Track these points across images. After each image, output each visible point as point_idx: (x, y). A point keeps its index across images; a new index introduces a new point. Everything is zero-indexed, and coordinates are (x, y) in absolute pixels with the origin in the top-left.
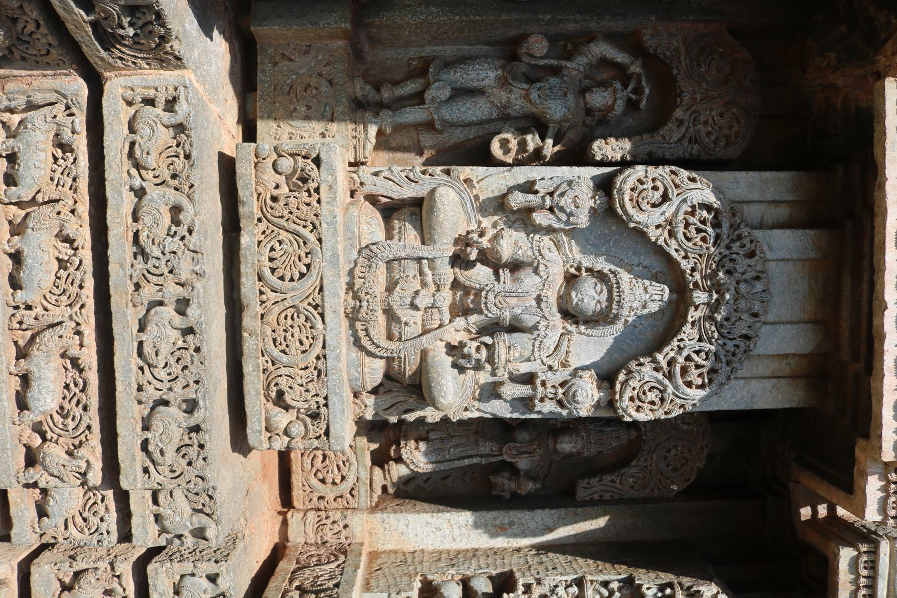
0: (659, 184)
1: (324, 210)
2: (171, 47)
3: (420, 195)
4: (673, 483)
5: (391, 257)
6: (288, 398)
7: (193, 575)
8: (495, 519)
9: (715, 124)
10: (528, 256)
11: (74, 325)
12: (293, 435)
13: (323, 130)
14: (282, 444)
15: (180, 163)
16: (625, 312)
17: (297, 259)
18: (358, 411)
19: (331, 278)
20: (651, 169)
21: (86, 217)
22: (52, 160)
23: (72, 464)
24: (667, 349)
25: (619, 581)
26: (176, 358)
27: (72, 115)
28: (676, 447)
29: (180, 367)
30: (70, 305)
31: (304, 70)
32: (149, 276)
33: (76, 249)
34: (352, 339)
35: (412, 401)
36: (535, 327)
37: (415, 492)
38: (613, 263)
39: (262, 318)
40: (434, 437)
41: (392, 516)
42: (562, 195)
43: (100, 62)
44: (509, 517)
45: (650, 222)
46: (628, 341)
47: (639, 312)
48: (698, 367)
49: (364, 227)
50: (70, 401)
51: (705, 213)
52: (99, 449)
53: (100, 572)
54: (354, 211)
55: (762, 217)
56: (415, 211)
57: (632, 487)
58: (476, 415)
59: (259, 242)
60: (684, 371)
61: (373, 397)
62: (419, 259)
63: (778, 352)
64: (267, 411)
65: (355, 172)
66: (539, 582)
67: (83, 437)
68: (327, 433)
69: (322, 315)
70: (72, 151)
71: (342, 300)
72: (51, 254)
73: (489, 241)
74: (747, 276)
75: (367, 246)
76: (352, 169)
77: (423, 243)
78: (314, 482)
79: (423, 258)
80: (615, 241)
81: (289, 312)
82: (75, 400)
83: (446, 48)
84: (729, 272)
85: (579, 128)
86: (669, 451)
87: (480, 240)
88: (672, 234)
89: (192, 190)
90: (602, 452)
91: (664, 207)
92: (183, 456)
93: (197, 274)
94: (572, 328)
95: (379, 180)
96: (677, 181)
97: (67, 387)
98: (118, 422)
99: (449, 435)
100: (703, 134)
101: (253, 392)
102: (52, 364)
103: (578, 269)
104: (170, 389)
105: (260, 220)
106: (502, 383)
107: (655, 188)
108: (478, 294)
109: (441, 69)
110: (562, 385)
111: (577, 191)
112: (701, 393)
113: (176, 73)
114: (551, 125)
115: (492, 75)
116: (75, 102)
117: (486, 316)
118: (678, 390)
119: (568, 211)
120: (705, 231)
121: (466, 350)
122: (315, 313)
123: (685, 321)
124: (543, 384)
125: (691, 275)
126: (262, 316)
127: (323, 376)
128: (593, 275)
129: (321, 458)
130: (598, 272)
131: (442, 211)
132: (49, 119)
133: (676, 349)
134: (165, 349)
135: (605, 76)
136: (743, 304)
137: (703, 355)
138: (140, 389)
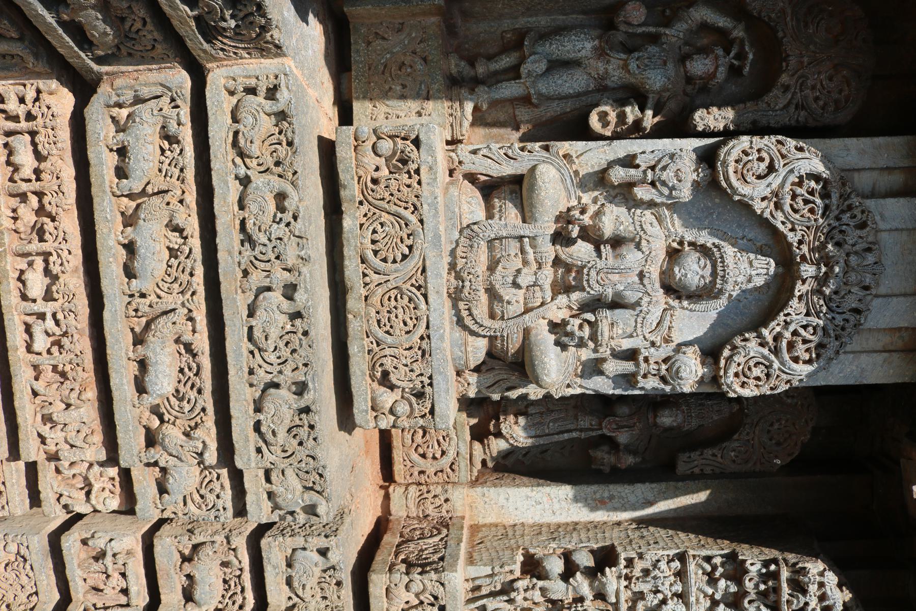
0: (764, 155)
1: (425, 191)
2: (272, 36)
3: (519, 172)
4: (776, 457)
5: (493, 236)
6: (393, 378)
7: (304, 549)
8: (595, 493)
9: (824, 88)
10: (629, 231)
11: (186, 311)
12: (399, 414)
13: (419, 109)
14: (388, 423)
15: (283, 150)
16: (729, 287)
17: (399, 240)
18: (461, 389)
19: (434, 259)
20: (756, 139)
21: (194, 206)
22: (159, 152)
23: (190, 445)
24: (773, 324)
25: (722, 556)
26: (285, 342)
27: (177, 107)
28: (779, 420)
29: (289, 350)
30: (182, 292)
31: (398, 49)
33: (186, 238)
34: (455, 319)
35: (514, 378)
36: (638, 303)
37: (514, 466)
38: (717, 236)
39: (366, 300)
40: (534, 412)
41: (492, 490)
42: (664, 168)
43: (202, 55)
44: (609, 491)
45: (755, 194)
46: (732, 316)
47: (744, 287)
48: (805, 341)
49: (465, 207)
50: (185, 385)
51: (813, 184)
52: (214, 430)
53: (217, 545)
54: (454, 191)
55: (874, 184)
56: (516, 188)
57: (734, 461)
58: (578, 391)
59: (361, 225)
60: (791, 346)
61: (476, 375)
62: (520, 238)
63: (890, 326)
64: (373, 391)
65: (453, 151)
66: (641, 556)
67: (198, 419)
68: (432, 412)
69: (425, 296)
70: (178, 142)
71: (445, 280)
72: (162, 244)
73: (591, 218)
74: (857, 248)
75: (468, 226)
76: (450, 147)
77: (524, 221)
78: (415, 457)
79: (524, 237)
80: (719, 213)
81: (393, 294)
82: (189, 384)
83: (539, 18)
84: (838, 244)
85: (679, 98)
86: (772, 425)
87: (581, 217)
88: (778, 206)
89: (296, 176)
90: (703, 425)
91: (770, 178)
92: (294, 437)
93: (302, 259)
94: (675, 303)
95: (478, 158)
96: (784, 151)
97: (181, 371)
98: (231, 405)
99: (548, 409)
100: (811, 99)
101: (358, 373)
102: (167, 350)
103: (681, 243)
104: (280, 372)
105: (361, 203)
106: (604, 360)
107: (761, 159)
108: (580, 270)
109: (536, 41)
110: (665, 361)
111: (679, 164)
112: (809, 368)
113: (276, 60)
114: (651, 96)
115: (589, 45)
116: (180, 94)
117: (588, 293)
118: (784, 365)
119: (670, 185)
120: (814, 202)
121: (569, 328)
122: (418, 293)
123: (792, 295)
124: (646, 360)
125: (798, 248)
126: (366, 297)
127: (427, 356)
128: (696, 249)
129: (421, 432)
130: (702, 246)
131: (543, 188)
132: (155, 112)
133: (782, 323)
134: (274, 333)
135: (705, 41)
136: (853, 277)
137: (811, 329)
138: (251, 372)
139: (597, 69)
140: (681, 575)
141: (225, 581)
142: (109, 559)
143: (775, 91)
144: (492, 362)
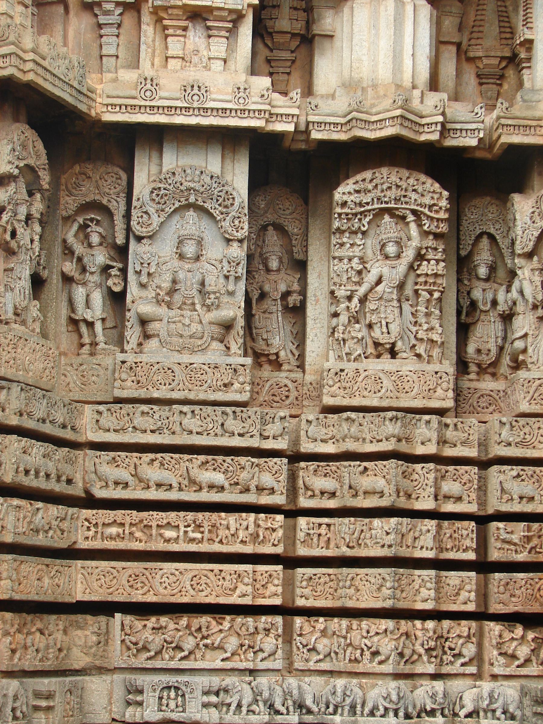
0: (140, 215)
6: (226, 382)
23: (248, 468)
24: (215, 215)
32: (170, 428)
48: (224, 201)
51: (154, 195)
69: (191, 364)
77: (161, 320)
78: (287, 402)
86: (280, 209)
91: (150, 213)
97: (215, 469)
100: (115, 191)
105: (147, 389)
107: (142, 217)
110: (229, 263)
124: (228, 271)
129: (274, 397)
136: (196, 179)
139: (92, 287)
140: (341, 259)
141: (325, 476)
142: (311, 532)
143: (110, 207)
144: (225, 343)
